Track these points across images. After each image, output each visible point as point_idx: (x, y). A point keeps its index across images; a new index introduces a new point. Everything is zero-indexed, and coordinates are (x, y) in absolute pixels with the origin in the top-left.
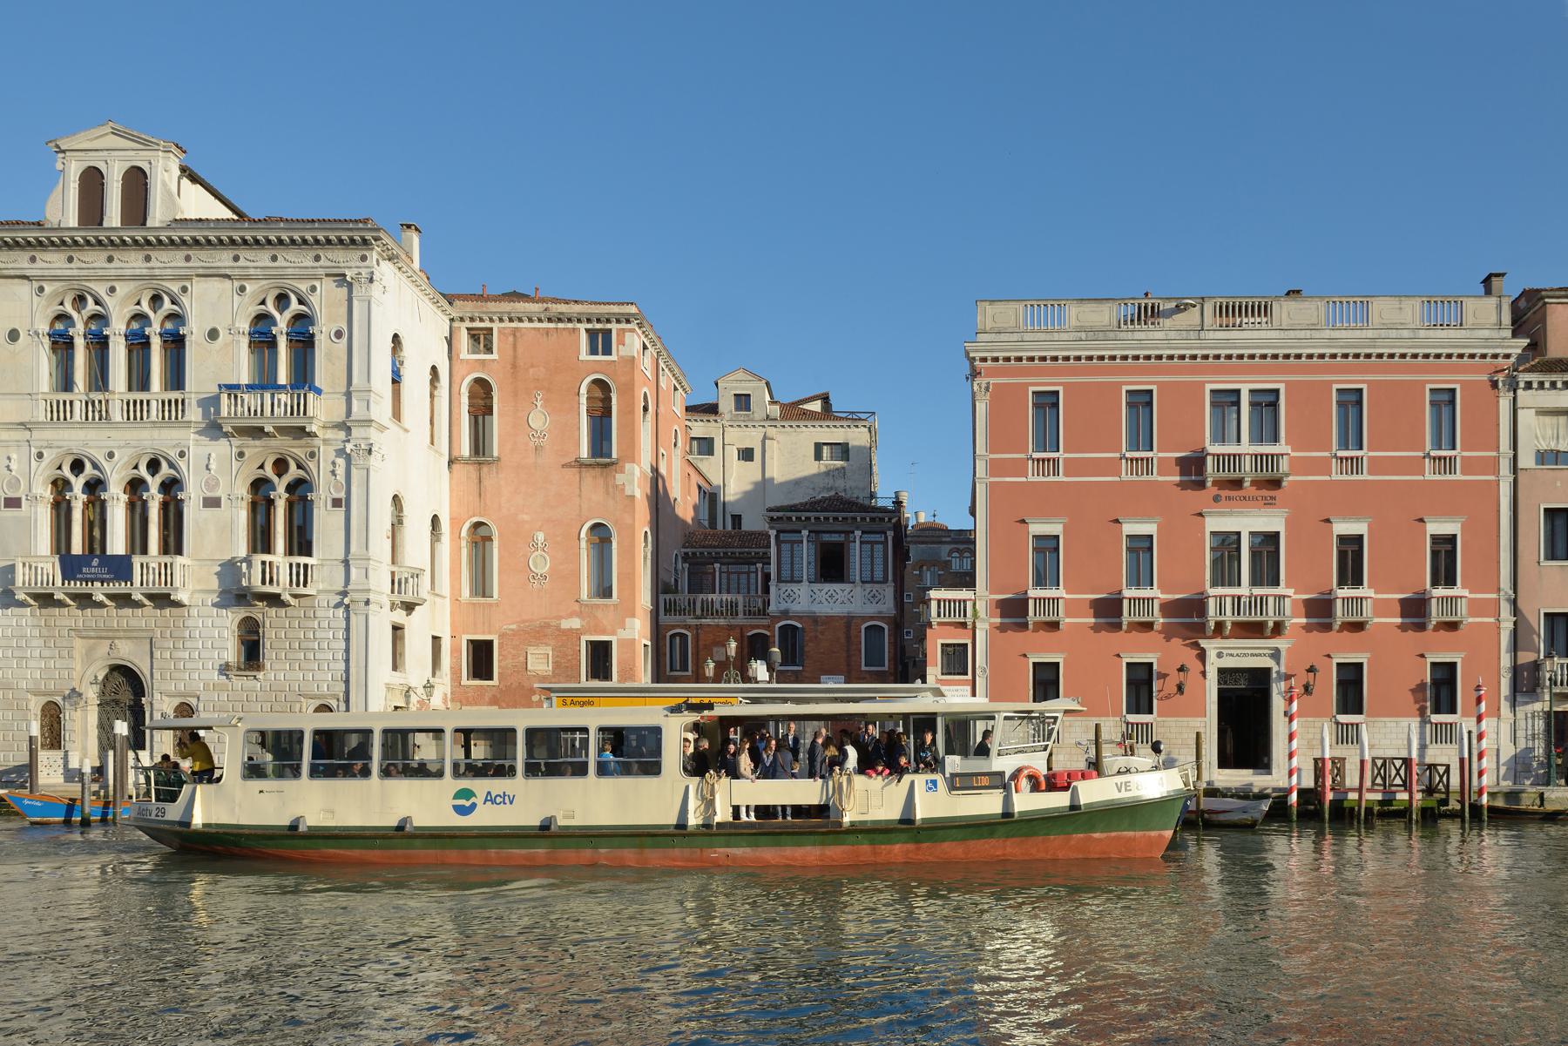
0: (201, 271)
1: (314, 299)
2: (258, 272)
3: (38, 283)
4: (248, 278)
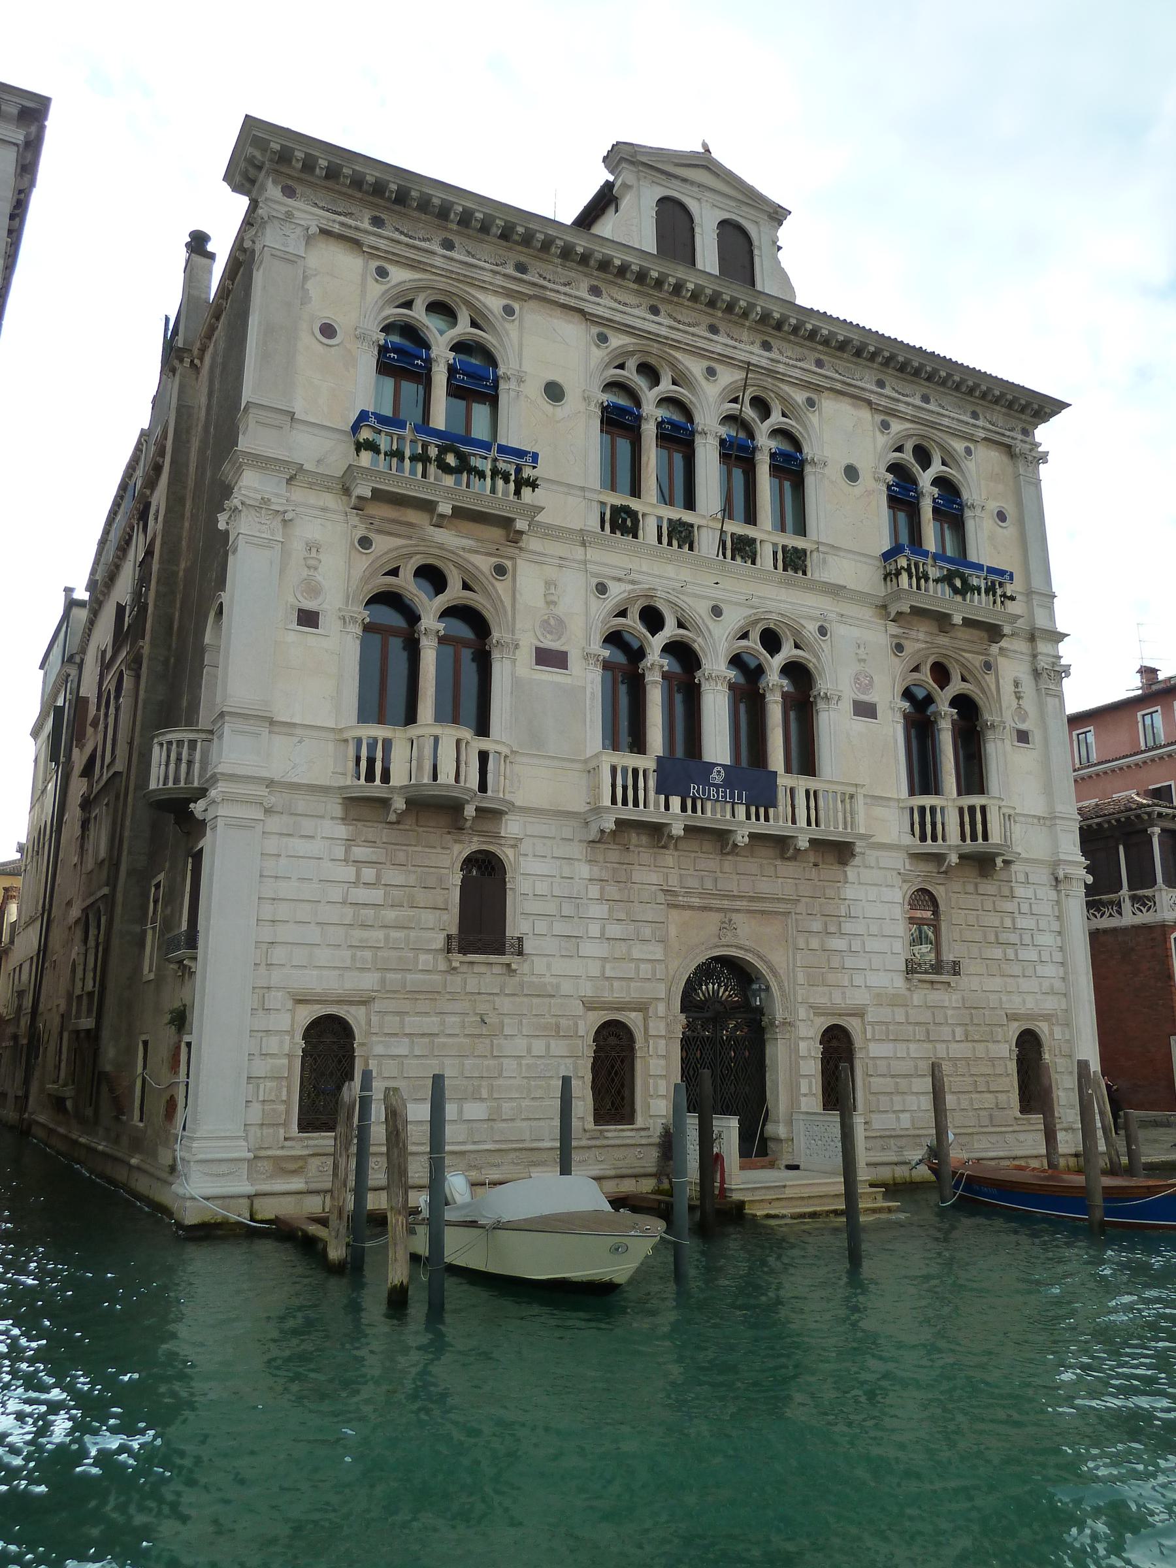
0: (839, 386)
1: (970, 465)
2: (910, 410)
3: (602, 328)
4: (892, 413)
